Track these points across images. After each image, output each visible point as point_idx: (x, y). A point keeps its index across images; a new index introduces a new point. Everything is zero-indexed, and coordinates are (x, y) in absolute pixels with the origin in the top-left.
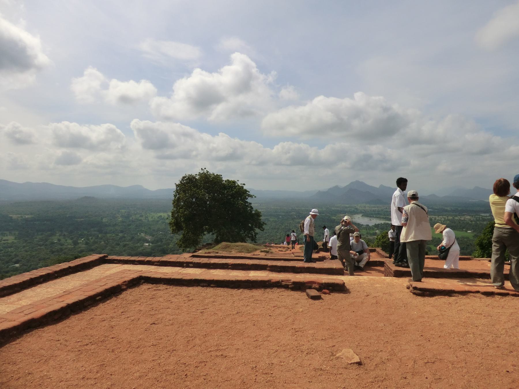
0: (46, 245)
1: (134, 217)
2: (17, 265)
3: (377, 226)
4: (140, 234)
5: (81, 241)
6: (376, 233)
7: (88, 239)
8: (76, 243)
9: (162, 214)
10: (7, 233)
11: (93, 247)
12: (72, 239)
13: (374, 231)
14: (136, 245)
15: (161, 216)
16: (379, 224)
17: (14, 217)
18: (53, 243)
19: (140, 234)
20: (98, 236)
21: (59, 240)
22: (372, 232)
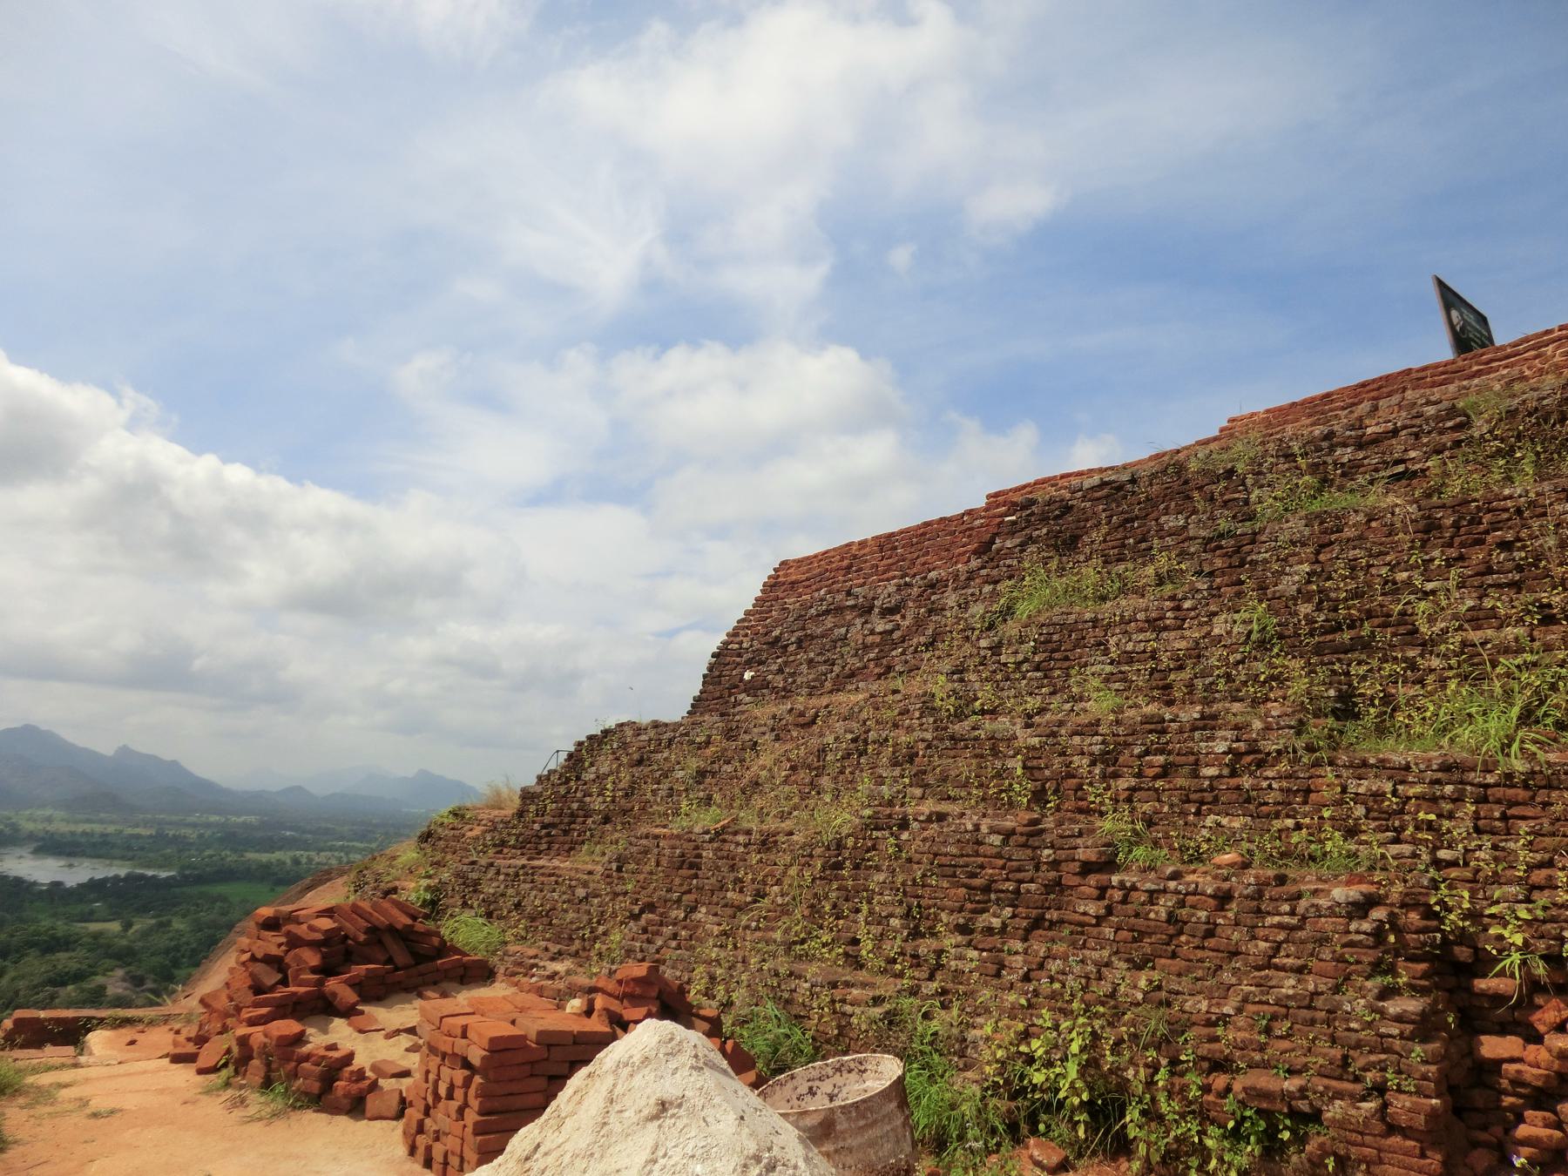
3: (94, 886)
16: (105, 880)
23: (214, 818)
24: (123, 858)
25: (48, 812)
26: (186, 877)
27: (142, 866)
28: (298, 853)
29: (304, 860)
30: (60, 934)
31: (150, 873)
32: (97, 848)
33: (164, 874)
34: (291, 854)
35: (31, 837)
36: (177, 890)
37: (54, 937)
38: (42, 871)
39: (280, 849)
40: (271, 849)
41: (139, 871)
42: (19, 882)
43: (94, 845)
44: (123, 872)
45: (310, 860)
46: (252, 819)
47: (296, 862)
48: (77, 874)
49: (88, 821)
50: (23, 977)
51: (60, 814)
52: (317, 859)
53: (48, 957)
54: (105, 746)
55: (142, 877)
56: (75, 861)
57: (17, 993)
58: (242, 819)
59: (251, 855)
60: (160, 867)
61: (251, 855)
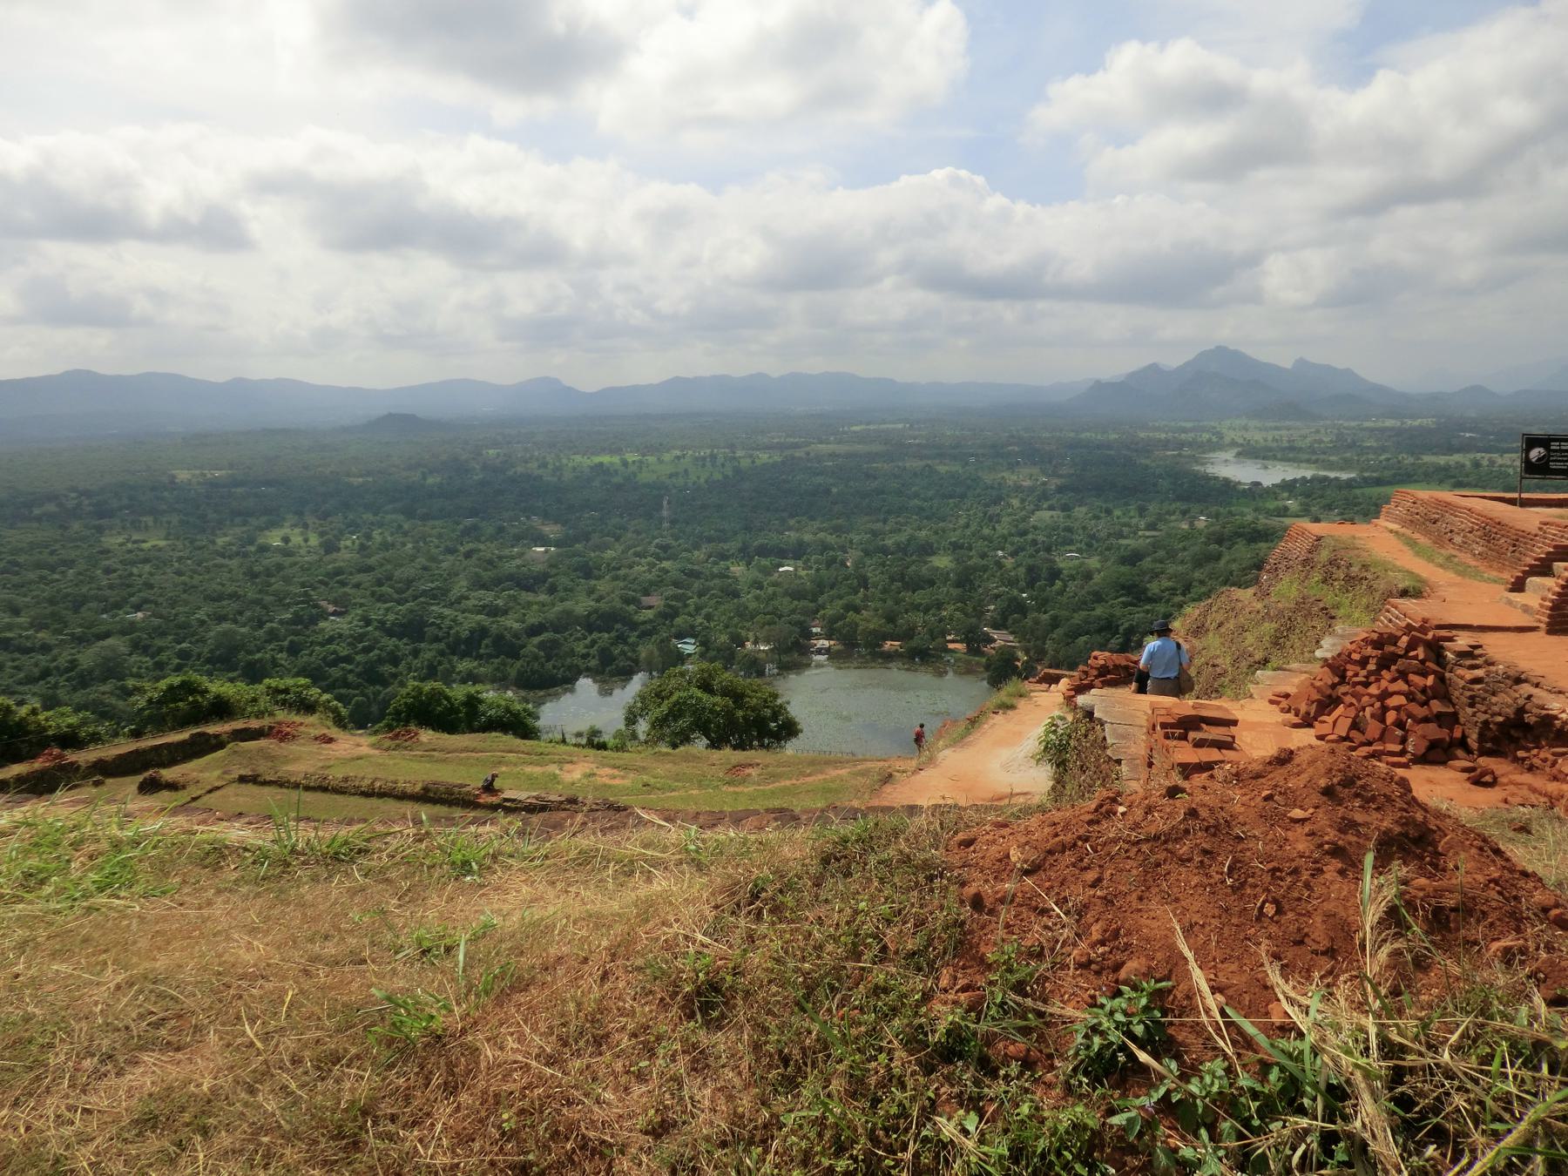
0: (245, 555)
1: (520, 469)
2: (140, 615)
3: (1288, 487)
4: (528, 518)
5: (349, 543)
6: (1286, 509)
7: (368, 537)
8: (330, 547)
9: (606, 459)
10: (149, 520)
11: (372, 561)
12: (322, 534)
13: (1280, 503)
14: (506, 552)
15: (601, 464)
16: (1295, 481)
17: (183, 475)
18: (264, 549)
19: (528, 518)
20: (400, 527)
21: (286, 540)
22: (1271, 505)
23: (1389, 423)
24: (1308, 461)
25: (1243, 421)
26: (1365, 479)
27: (1325, 469)
28: (1479, 455)
29: (1485, 463)
30: (1260, 528)
31: (1332, 475)
32: (1289, 453)
33: (1344, 476)
34: (1472, 456)
35: (1233, 444)
36: (1358, 492)
37: (1256, 531)
38: (1244, 473)
39: (1458, 451)
40: (1450, 450)
41: (1322, 473)
42: (1227, 481)
43: (1283, 449)
44: (1309, 474)
45: (1492, 463)
46: (1428, 422)
47: (1477, 465)
48: (1272, 475)
49: (1277, 428)
50: (1235, 560)
51: (1253, 423)
52: (1500, 461)
53: (1253, 546)
54: (1285, 359)
55: (1326, 478)
56: (1269, 463)
57: (1231, 573)
58: (1417, 423)
59: (1427, 459)
60: (1342, 469)
61: (1427, 459)
